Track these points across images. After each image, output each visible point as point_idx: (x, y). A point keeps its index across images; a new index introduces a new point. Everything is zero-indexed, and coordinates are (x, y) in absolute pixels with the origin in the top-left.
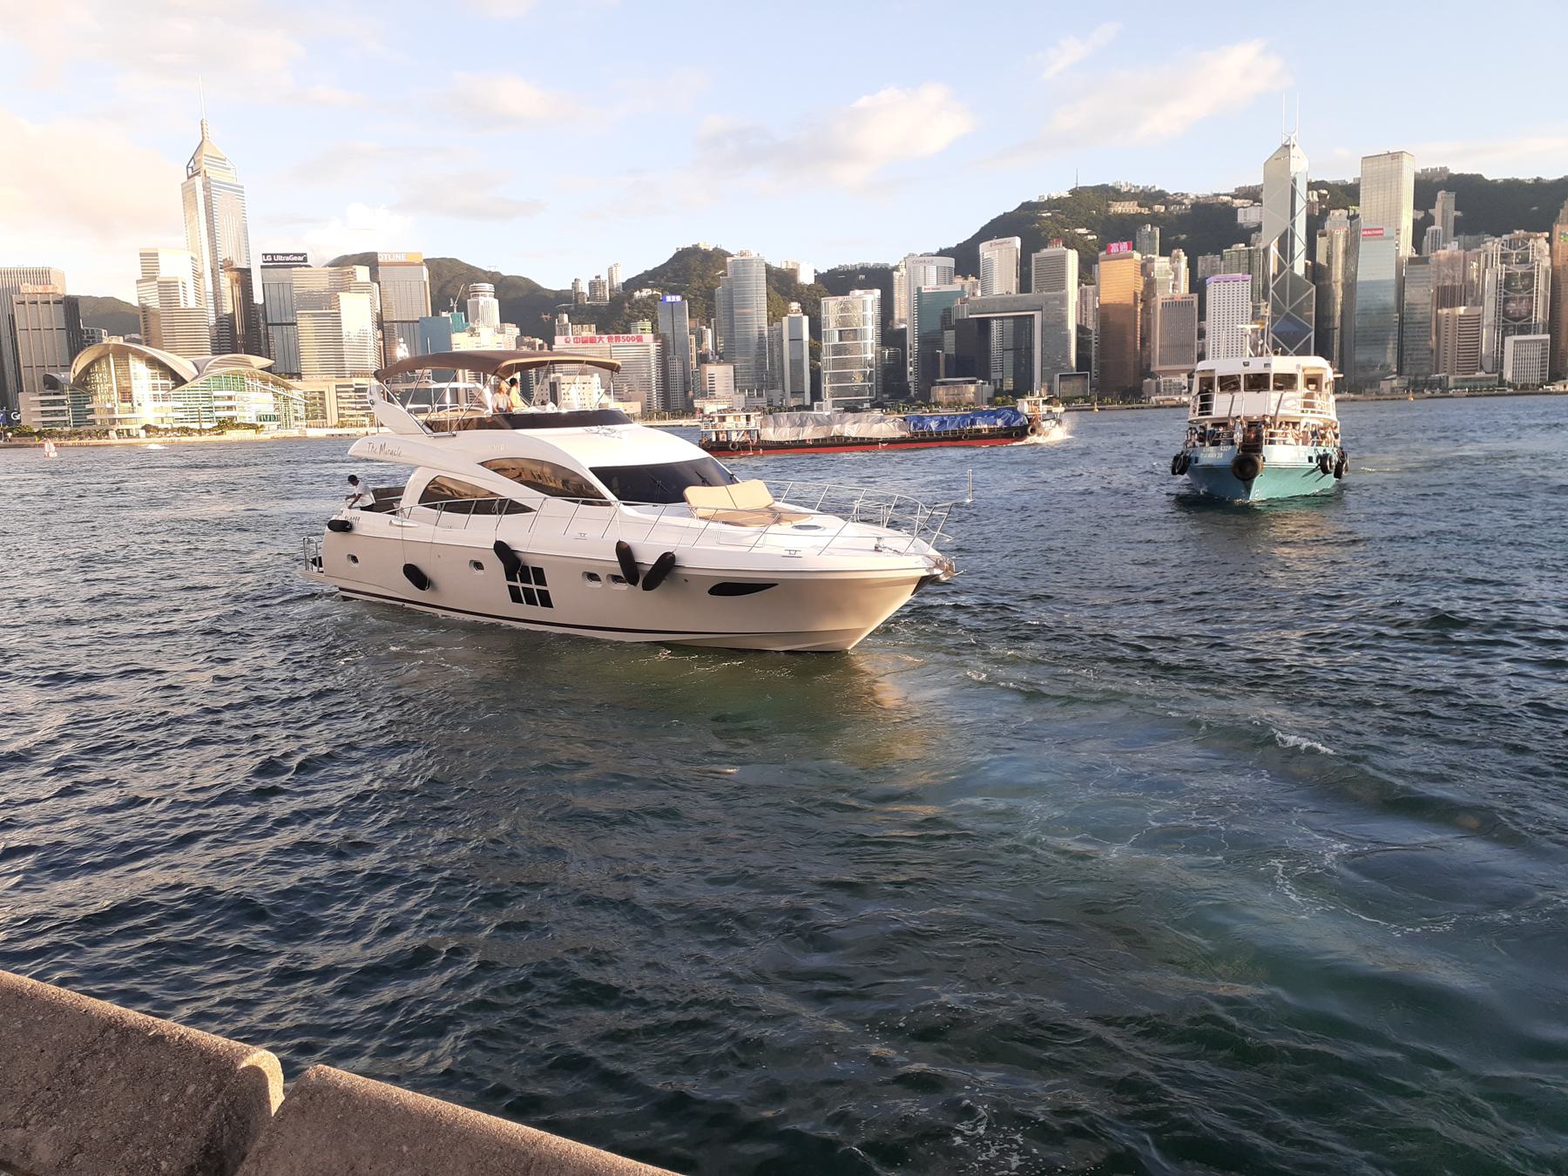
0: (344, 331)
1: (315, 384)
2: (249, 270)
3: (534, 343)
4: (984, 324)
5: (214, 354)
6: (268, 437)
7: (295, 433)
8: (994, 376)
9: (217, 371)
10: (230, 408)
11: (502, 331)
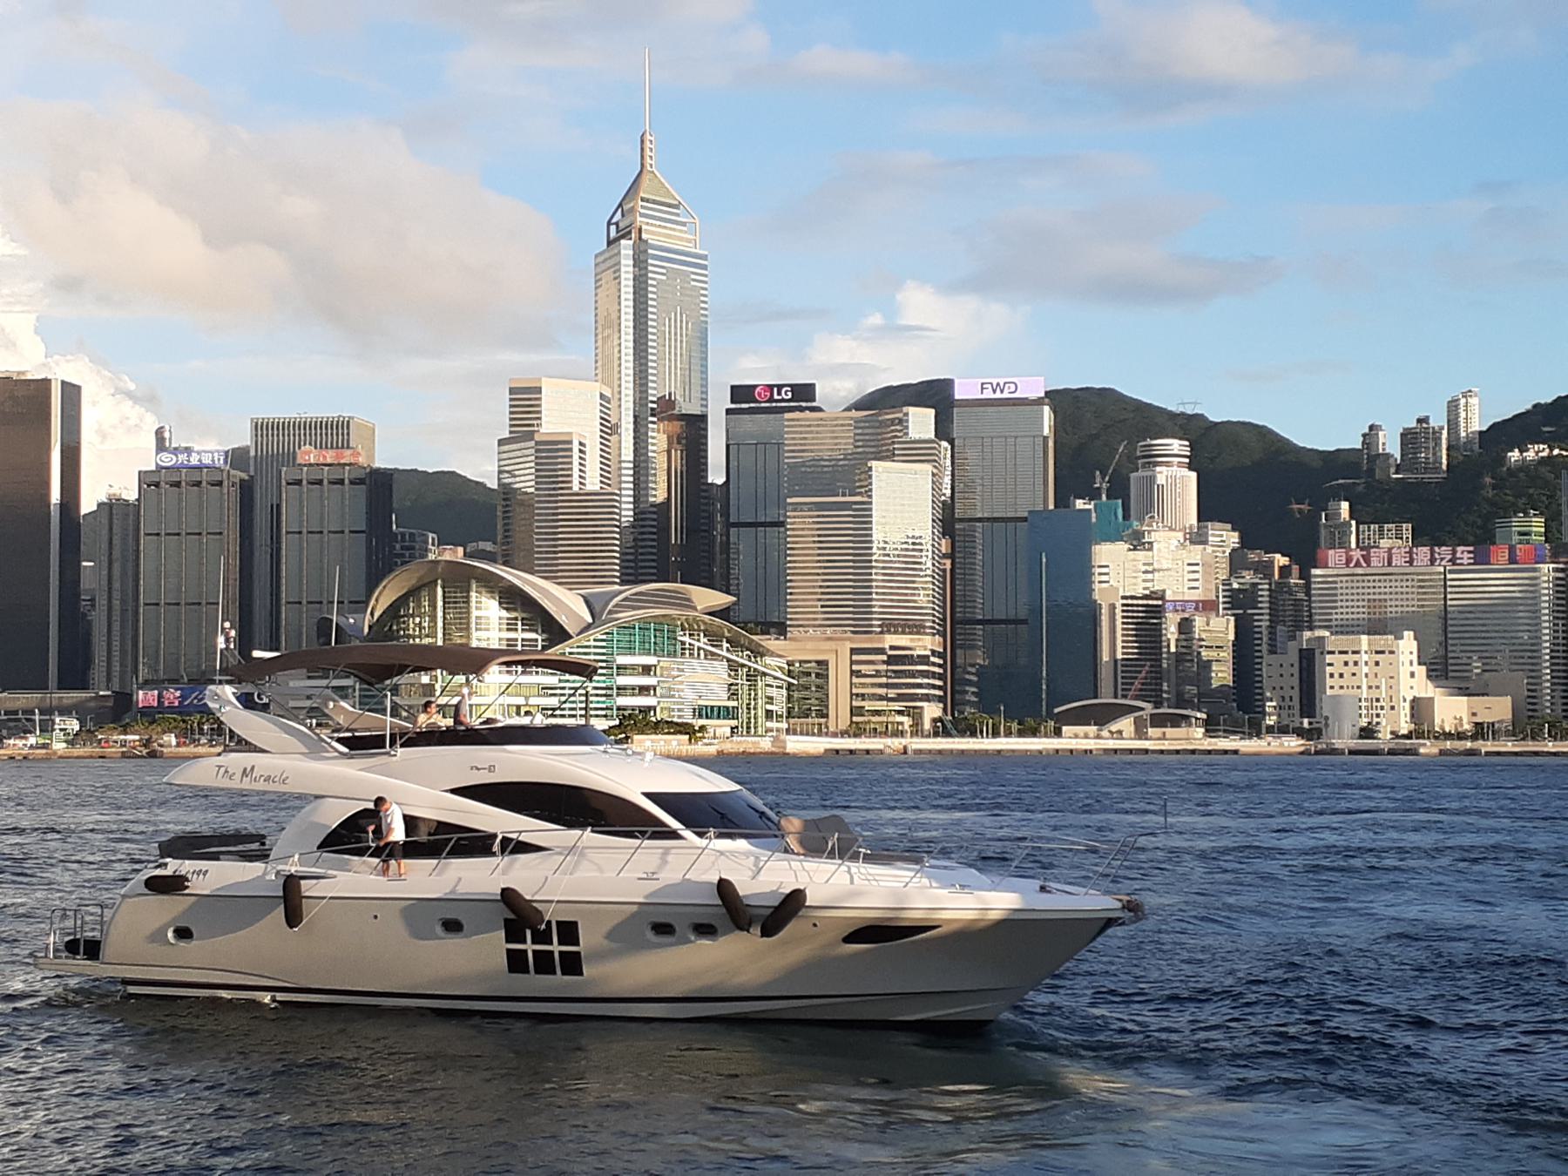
0: (877, 535)
1: (810, 645)
2: (703, 418)
3: (1272, 562)
5: (623, 583)
6: (712, 750)
7: (765, 744)
9: (625, 616)
10: (644, 690)
11: (1198, 538)
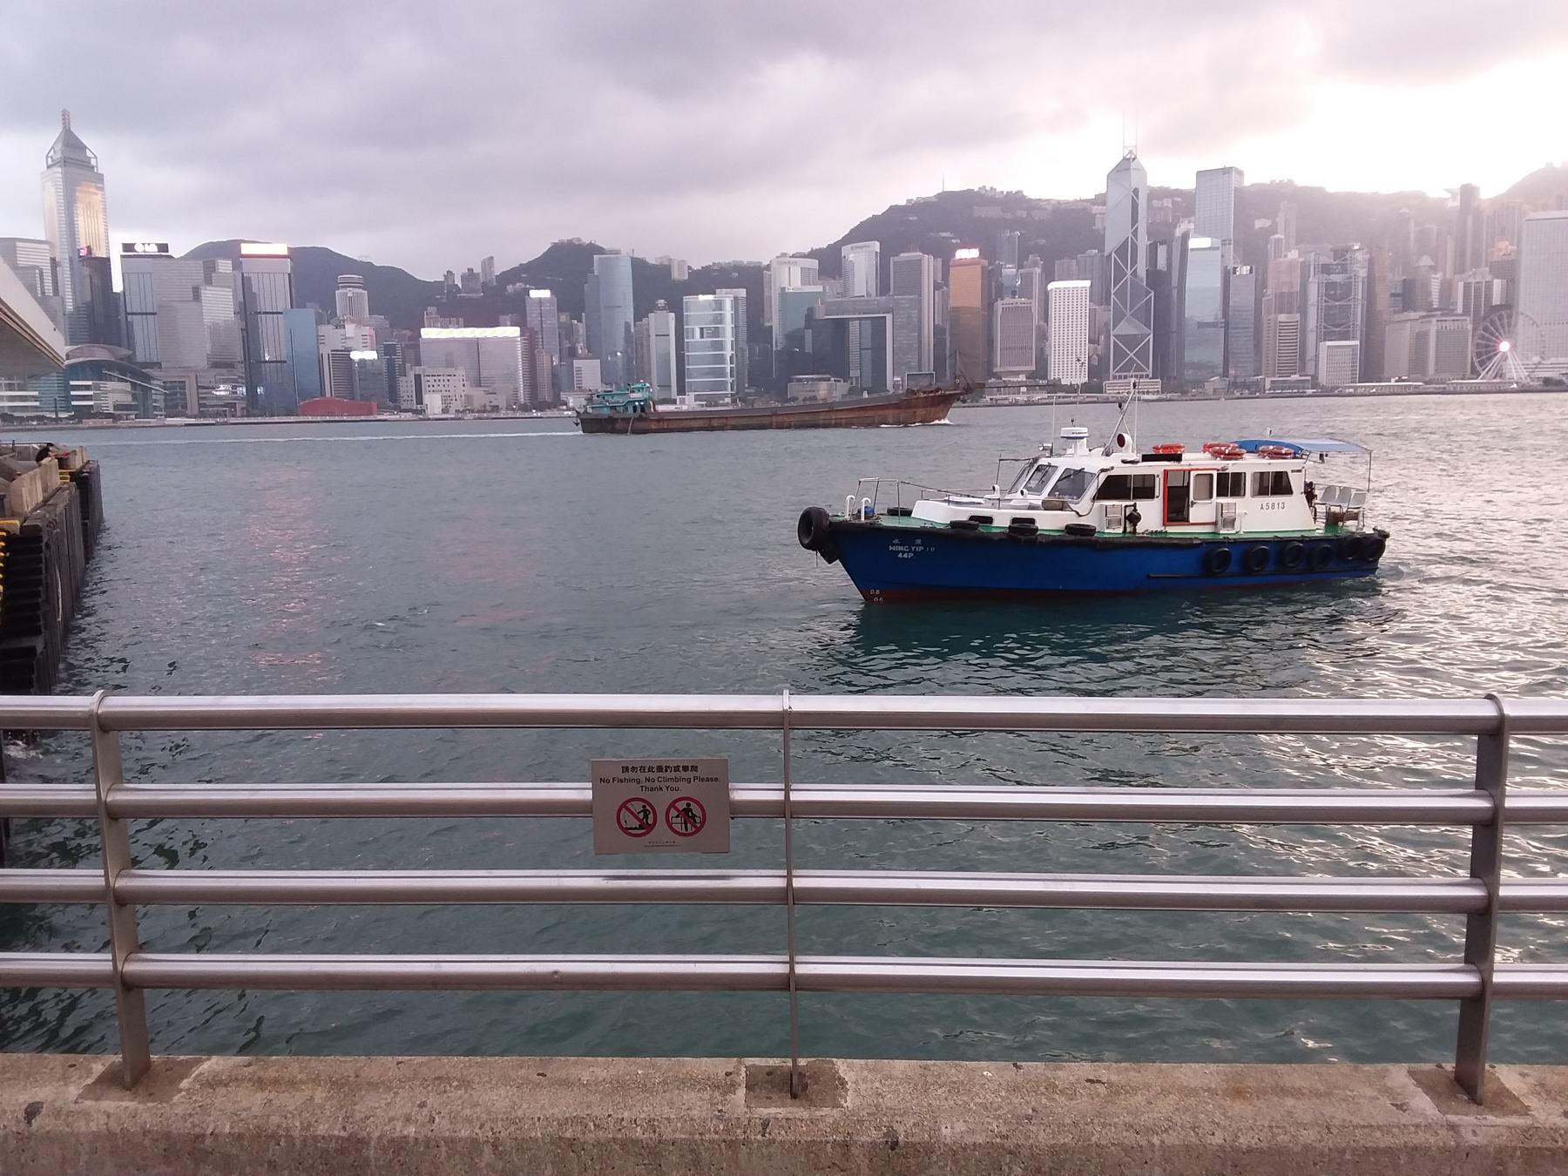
4: (841, 325)
8: (854, 373)
